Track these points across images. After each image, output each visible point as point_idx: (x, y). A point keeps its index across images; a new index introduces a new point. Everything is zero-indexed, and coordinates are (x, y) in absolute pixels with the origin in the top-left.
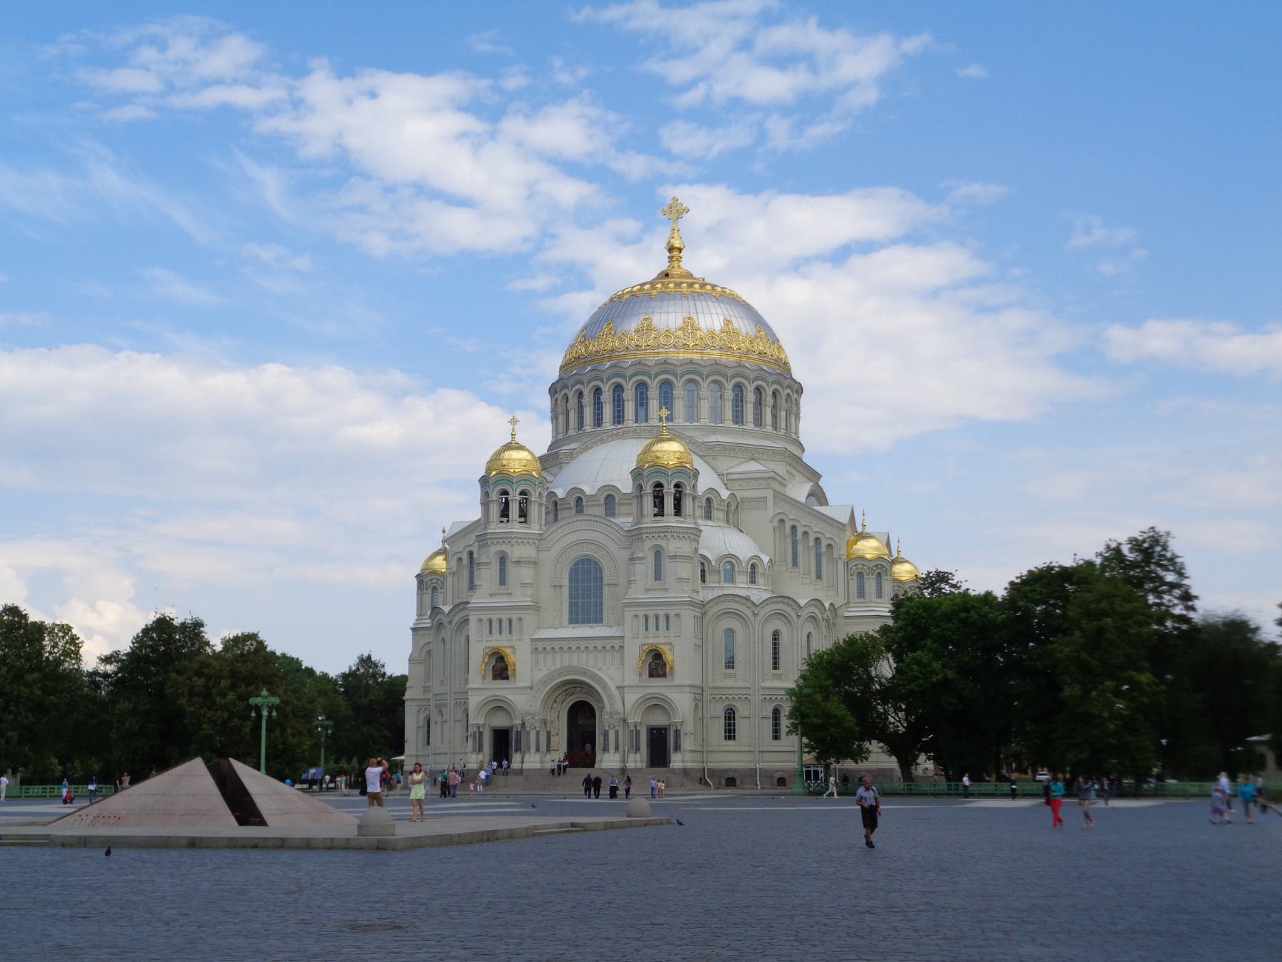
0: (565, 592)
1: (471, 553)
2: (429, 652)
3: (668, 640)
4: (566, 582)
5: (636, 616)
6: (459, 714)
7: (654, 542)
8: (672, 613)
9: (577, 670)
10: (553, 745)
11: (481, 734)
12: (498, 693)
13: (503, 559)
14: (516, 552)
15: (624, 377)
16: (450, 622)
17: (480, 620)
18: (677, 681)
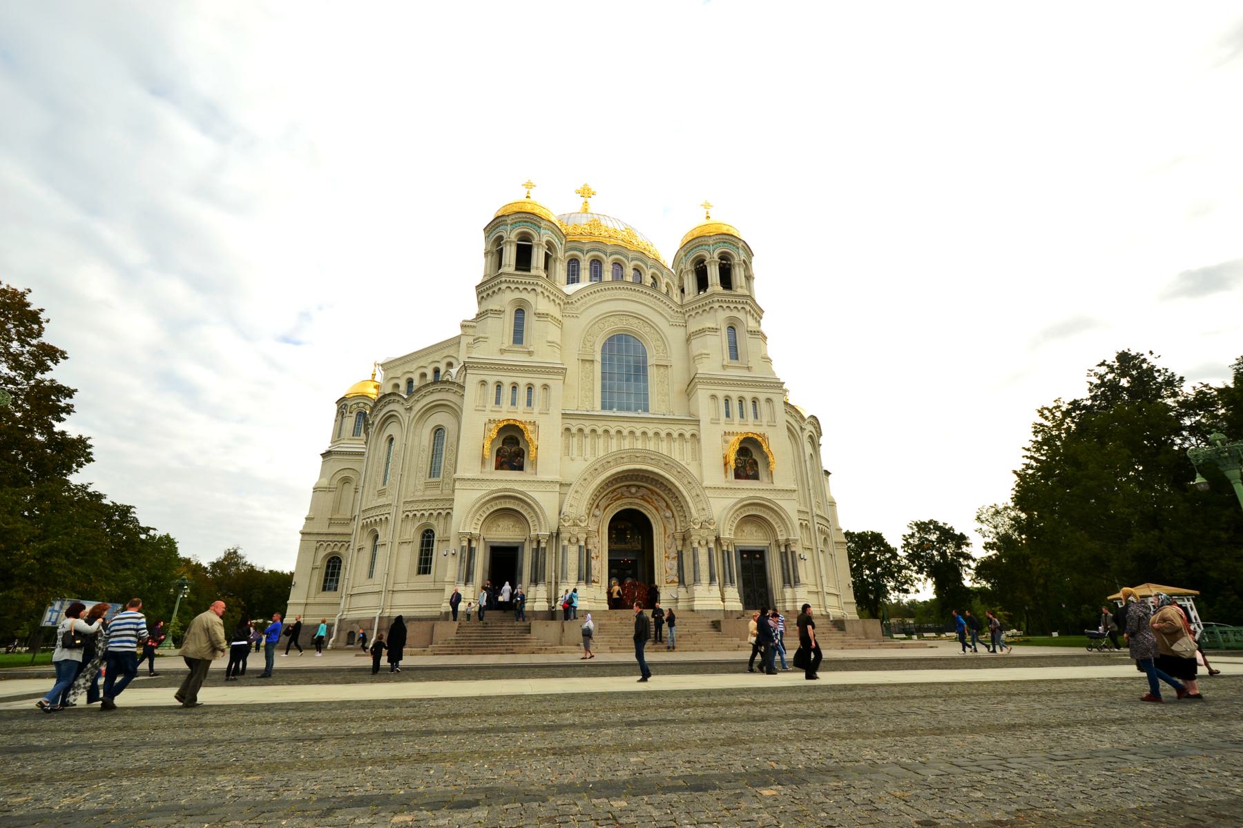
0: (598, 367)
1: (410, 382)
2: (346, 480)
3: (758, 430)
4: (598, 357)
5: (714, 397)
6: (412, 533)
7: (728, 313)
8: (762, 397)
9: (646, 456)
10: (594, 572)
11: (471, 551)
12: (508, 486)
13: (520, 313)
14: (541, 304)
15: (581, 251)
16: (411, 409)
17: (483, 383)
18: (778, 484)
